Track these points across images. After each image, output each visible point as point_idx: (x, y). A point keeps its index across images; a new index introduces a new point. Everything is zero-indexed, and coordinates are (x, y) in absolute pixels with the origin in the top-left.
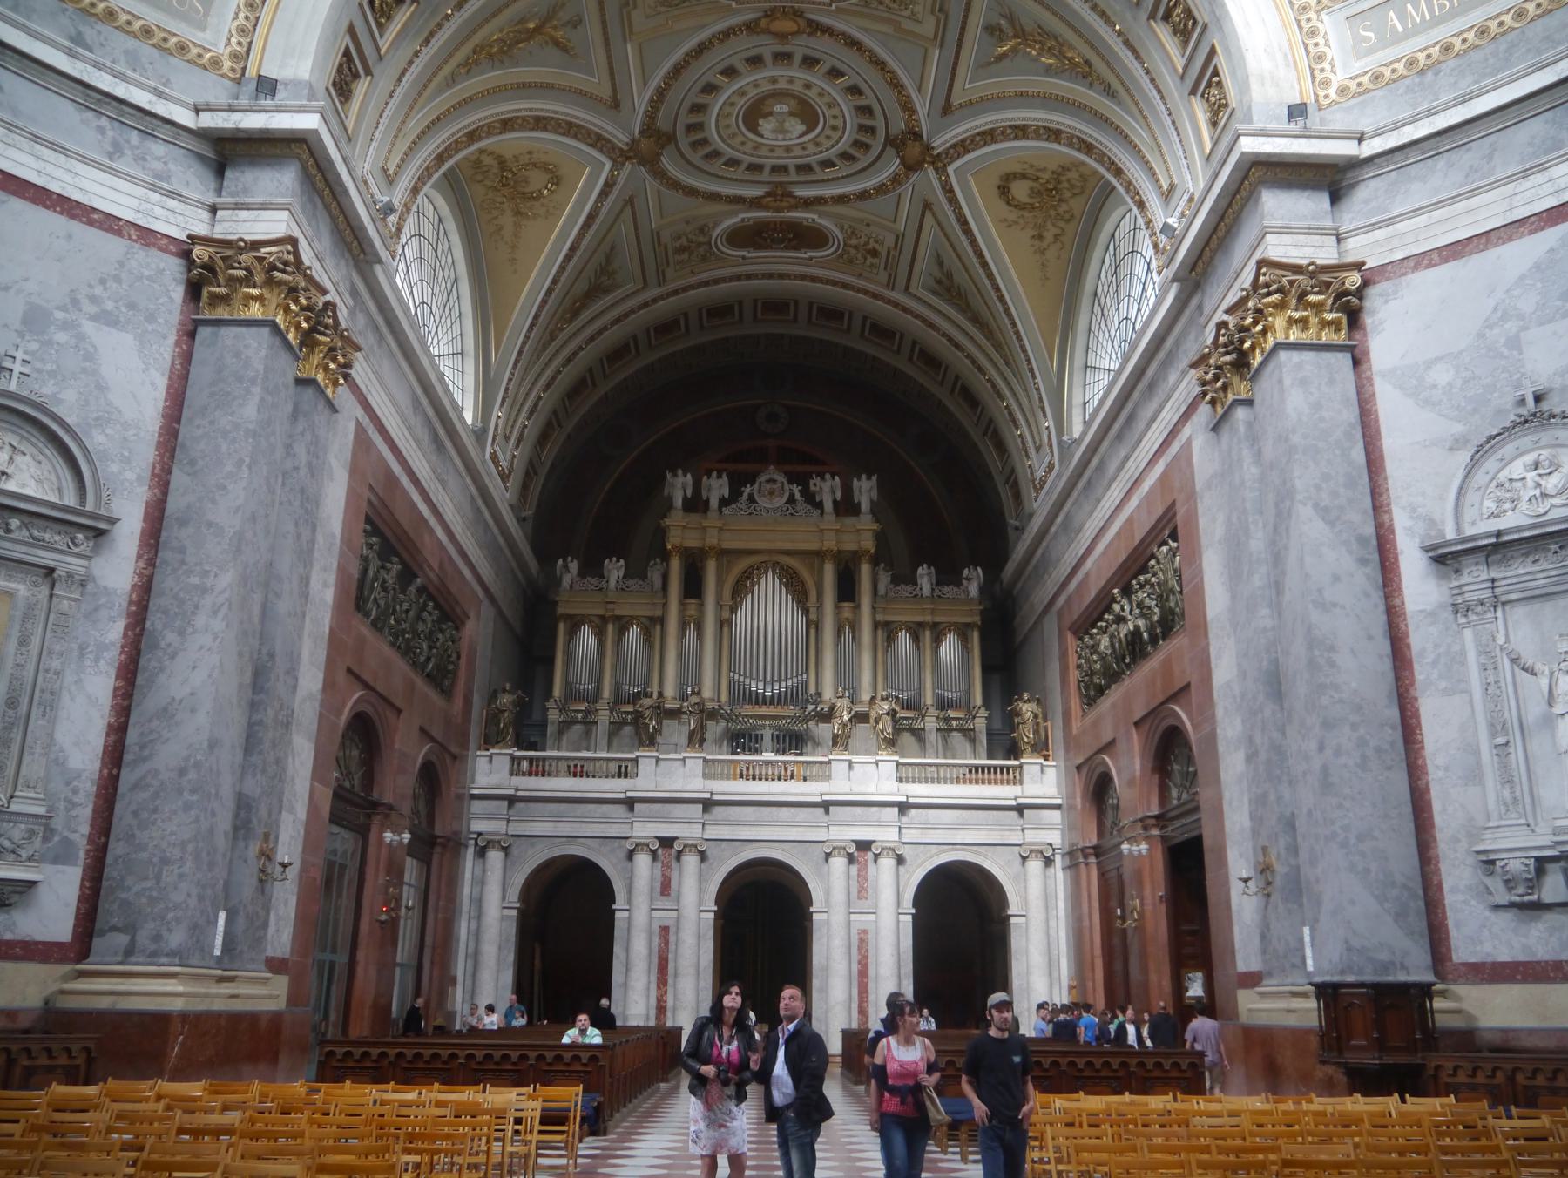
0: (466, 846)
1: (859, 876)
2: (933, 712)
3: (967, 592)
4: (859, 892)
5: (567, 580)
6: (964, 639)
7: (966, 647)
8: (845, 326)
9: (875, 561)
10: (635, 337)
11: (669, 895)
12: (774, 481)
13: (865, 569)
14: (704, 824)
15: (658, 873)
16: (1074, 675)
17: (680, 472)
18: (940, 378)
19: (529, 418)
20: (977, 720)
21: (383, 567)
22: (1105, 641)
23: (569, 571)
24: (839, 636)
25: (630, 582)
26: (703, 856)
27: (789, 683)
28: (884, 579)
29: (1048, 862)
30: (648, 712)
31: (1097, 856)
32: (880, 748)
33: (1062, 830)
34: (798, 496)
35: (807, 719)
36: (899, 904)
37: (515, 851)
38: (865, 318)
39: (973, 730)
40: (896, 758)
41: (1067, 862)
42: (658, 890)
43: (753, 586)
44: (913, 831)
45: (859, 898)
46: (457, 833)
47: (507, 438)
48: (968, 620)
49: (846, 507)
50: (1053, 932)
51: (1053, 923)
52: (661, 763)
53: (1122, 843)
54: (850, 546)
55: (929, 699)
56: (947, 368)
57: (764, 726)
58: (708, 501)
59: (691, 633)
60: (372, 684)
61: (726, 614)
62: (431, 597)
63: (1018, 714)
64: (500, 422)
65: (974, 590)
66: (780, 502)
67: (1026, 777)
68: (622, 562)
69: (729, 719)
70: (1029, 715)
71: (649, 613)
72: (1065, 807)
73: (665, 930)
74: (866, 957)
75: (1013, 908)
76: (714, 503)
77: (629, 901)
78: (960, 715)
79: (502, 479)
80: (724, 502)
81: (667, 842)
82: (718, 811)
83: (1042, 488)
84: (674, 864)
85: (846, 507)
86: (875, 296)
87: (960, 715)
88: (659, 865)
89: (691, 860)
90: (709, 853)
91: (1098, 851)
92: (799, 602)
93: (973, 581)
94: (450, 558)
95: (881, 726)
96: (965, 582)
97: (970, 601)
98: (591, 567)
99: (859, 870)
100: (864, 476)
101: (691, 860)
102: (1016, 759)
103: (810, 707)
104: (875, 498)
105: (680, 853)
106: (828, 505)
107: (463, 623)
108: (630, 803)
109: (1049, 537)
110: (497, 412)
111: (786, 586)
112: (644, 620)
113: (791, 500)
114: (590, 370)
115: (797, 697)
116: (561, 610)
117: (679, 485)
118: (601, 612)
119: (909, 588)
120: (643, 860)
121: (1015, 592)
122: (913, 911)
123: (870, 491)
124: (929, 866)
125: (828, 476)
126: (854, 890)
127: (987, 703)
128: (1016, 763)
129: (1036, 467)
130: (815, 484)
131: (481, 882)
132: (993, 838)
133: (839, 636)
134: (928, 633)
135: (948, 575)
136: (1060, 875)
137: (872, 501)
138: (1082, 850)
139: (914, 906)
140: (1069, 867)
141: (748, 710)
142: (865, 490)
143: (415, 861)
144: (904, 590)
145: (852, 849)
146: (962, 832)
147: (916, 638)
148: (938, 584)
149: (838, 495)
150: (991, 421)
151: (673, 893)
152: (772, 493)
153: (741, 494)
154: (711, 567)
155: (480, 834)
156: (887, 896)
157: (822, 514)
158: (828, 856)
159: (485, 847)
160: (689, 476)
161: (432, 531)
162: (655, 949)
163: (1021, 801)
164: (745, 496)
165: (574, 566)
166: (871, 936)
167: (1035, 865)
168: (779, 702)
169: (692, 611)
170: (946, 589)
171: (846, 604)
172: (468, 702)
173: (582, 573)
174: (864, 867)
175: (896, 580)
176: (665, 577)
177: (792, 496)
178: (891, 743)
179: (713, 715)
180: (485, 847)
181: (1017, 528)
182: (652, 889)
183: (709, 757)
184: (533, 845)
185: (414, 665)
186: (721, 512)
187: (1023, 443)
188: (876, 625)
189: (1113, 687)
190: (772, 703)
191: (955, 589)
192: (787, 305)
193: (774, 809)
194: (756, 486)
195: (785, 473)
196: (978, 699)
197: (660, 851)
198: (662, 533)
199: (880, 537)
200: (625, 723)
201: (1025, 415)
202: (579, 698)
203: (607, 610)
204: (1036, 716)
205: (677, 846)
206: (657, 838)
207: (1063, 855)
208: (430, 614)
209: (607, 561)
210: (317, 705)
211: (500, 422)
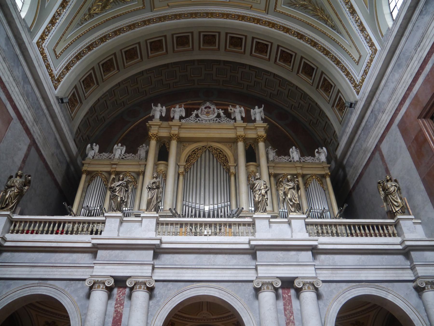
1: (285, 310)
3: (318, 159)
5: (91, 154)
8: (243, 50)
12: (210, 108)
13: (261, 145)
14: (153, 268)
17: (159, 105)
18: (291, 68)
25: (128, 155)
26: (151, 290)
27: (220, 205)
28: (272, 155)
30: (118, 189)
34: (222, 114)
38: (253, 38)
48: (323, 173)
52: (124, 224)
54: (251, 134)
65: (323, 157)
67: (404, 229)
71: (136, 170)
76: (177, 117)
80: (181, 118)
82: (166, 259)
84: (126, 302)
85: (247, 119)
86: (258, 21)
88: (113, 303)
90: (156, 292)
95: (289, 196)
99: (285, 305)
100: (257, 107)
105: (132, 289)
106: (238, 118)
109: (378, 92)
112: (133, 174)
113: (219, 116)
118: (108, 169)
119: (286, 158)
121: (345, 162)
123: (260, 112)
124: (343, 300)
130: (230, 109)
144: (284, 159)
145: (279, 284)
149: (244, 115)
152: (208, 113)
153: (192, 114)
154: (174, 145)
158: (257, 291)
164: (194, 115)
165: (96, 148)
169: (162, 167)
171: (251, 163)
173: (100, 151)
174: (288, 303)
176: (147, 153)
188: (270, 175)
191: (312, 158)
193: (212, 256)
194: (200, 111)
197: (115, 291)
203: (112, 168)
209: (116, 146)
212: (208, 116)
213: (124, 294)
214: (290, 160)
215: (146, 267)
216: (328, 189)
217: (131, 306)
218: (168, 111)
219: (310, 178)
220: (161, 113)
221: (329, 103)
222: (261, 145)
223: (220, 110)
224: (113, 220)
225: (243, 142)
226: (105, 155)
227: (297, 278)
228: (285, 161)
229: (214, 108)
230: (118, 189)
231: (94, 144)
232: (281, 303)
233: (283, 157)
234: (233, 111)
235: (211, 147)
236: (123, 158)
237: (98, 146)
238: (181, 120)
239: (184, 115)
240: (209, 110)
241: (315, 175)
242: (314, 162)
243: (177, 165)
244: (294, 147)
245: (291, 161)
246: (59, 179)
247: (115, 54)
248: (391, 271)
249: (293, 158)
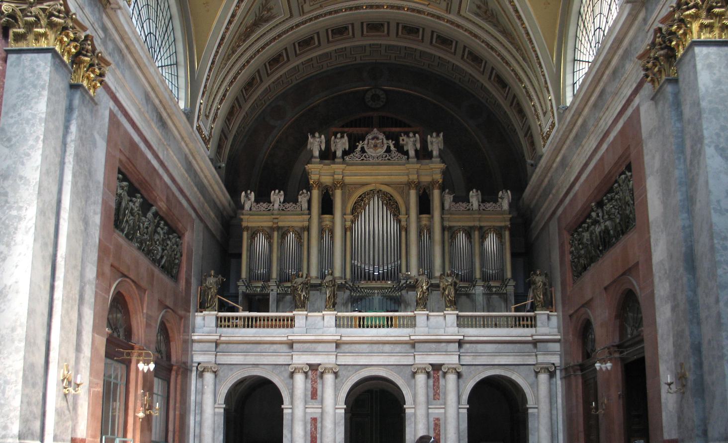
0: (191, 371)
1: (434, 385)
2: (480, 283)
3: (501, 206)
4: (434, 395)
6: (500, 236)
7: (501, 242)
9: (442, 188)
10: (286, 49)
11: (316, 399)
12: (377, 138)
13: (436, 193)
15: (309, 386)
16: (568, 258)
17: (317, 135)
19: (220, 104)
20: (508, 288)
21: (131, 201)
22: (586, 235)
23: (248, 199)
24: (420, 236)
25: (287, 205)
26: (336, 374)
28: (448, 198)
29: (552, 375)
30: (300, 287)
31: (582, 370)
32: (447, 307)
33: (560, 355)
34: (392, 148)
35: (400, 289)
36: (459, 402)
37: (221, 374)
39: (506, 294)
40: (457, 312)
41: (564, 374)
42: (310, 396)
43: (365, 205)
44: (468, 358)
45: (434, 399)
46: (185, 363)
47: (207, 117)
48: (503, 224)
49: (423, 154)
50: (554, 418)
51: (554, 412)
53: (596, 363)
54: (425, 179)
55: (478, 275)
56: (486, 62)
57: (374, 293)
58: (335, 152)
59: (326, 236)
60: (126, 273)
62: (162, 218)
63: (534, 283)
64: (202, 106)
65: (505, 205)
66: (381, 151)
67: (539, 323)
68: (282, 192)
69: (352, 289)
70: (540, 284)
72: (562, 340)
73: (314, 420)
74: (439, 435)
75: (531, 402)
76: (339, 153)
77: (292, 403)
78: (497, 284)
79: (205, 143)
80: (345, 153)
81: (313, 367)
82: (345, 348)
83: (548, 139)
84: (319, 381)
87: (497, 284)
89: (329, 378)
90: (340, 373)
91: (582, 367)
92: (394, 215)
93: (505, 199)
94: (173, 193)
95: (447, 292)
96: (500, 200)
97: (502, 213)
98: (263, 197)
100: (434, 135)
101: (329, 378)
102: (533, 312)
103: (403, 282)
104: (442, 147)
105: (322, 373)
106: (412, 153)
107: (183, 234)
108: (291, 344)
110: (200, 100)
111: (386, 205)
113: (388, 150)
114: (258, 71)
115: (393, 275)
116: (244, 224)
117: (316, 144)
118: (270, 224)
119: (465, 205)
120: (299, 378)
121: (532, 206)
122: (468, 406)
124: (478, 379)
125: (411, 135)
126: (431, 395)
127: (514, 277)
128: (532, 314)
129: (544, 126)
131: (201, 392)
132: (518, 360)
133: (420, 236)
134: (477, 233)
135: (489, 196)
136: (559, 382)
137: (440, 149)
138: (572, 367)
139: (468, 403)
140: (565, 378)
141: (363, 284)
142: (435, 143)
143: (160, 380)
144: (462, 206)
145: (430, 369)
146: (499, 357)
147: (469, 236)
148: (483, 201)
149: (418, 146)
150: (515, 96)
151: (319, 398)
152: (375, 146)
155: (199, 364)
156: (452, 397)
157: (408, 158)
158: (414, 374)
159: (203, 371)
160: (323, 136)
161: (161, 178)
162: (309, 432)
163: (535, 337)
164: (359, 149)
166: (442, 422)
167: (543, 377)
168: (383, 279)
170: (488, 205)
172: (188, 283)
173: (257, 201)
174: (436, 381)
176: (309, 202)
177: (389, 147)
178: (454, 304)
179: (341, 287)
180: (203, 371)
181: (532, 165)
182: (306, 395)
183: (340, 314)
184: (231, 370)
185: (155, 261)
186: (344, 159)
187: (535, 110)
188: (443, 229)
189: (592, 265)
190: (379, 279)
191: (494, 205)
192: (382, 25)
193: (381, 345)
194: (366, 142)
195: (384, 133)
196: (509, 274)
197: (310, 373)
199: (445, 173)
200: (286, 294)
201: (536, 92)
202: (258, 279)
204: (545, 284)
205: (320, 370)
206: (307, 364)
207: (561, 370)
208: (162, 229)
209: (273, 192)
210: (94, 287)
211: (202, 106)
212: (375, 150)
213: (316, 374)
214: (468, 208)
215: (331, 357)
216: (505, 243)
217: (323, 384)
218: (328, 143)
219: (487, 230)
220: (320, 147)
221: (522, 129)
222: (436, 193)
223: (390, 141)
224: (300, 317)
225: (416, 189)
226: (264, 206)
227: (444, 364)
229: (383, 139)
230: (300, 287)
231: (249, 191)
232: (431, 382)
233: (461, 203)
234: (404, 142)
235: (381, 190)
236: (283, 210)
238: (345, 157)
239: (347, 148)
244: (474, 190)
245: (469, 209)
246: (218, 238)
248: (519, 357)
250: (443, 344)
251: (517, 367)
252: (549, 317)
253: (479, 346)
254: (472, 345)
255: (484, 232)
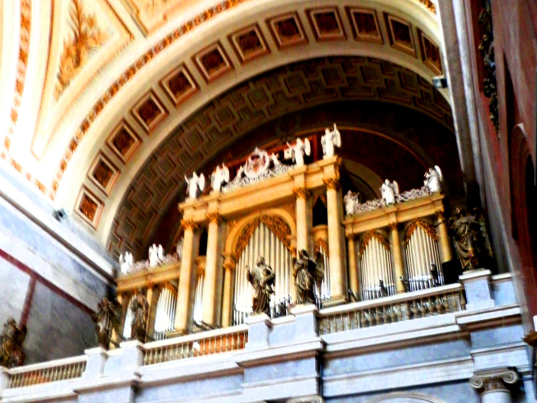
13: (331, 195)
17: (195, 174)
34: (276, 162)
54: (316, 181)
61: (228, 261)
66: (263, 169)
80: (224, 184)
113: (272, 166)
119: (374, 203)
144: (372, 205)
148: (402, 190)
170: (408, 194)
175: (363, 200)
191: (418, 191)
194: (246, 166)
198: (180, 215)
214: (379, 205)
222: (331, 195)
228: (371, 208)
229: (264, 157)
233: (369, 202)
237: (160, 247)
239: (227, 179)
240: (258, 160)
241: (420, 219)
242: (419, 197)
243: (220, 255)
245: (381, 207)
247: (124, 121)
248: (438, 369)
249: (385, 200)
250: (290, 364)
251: (436, 389)
252: (493, 287)
253: (359, 360)
254: (345, 360)
255: (406, 231)
